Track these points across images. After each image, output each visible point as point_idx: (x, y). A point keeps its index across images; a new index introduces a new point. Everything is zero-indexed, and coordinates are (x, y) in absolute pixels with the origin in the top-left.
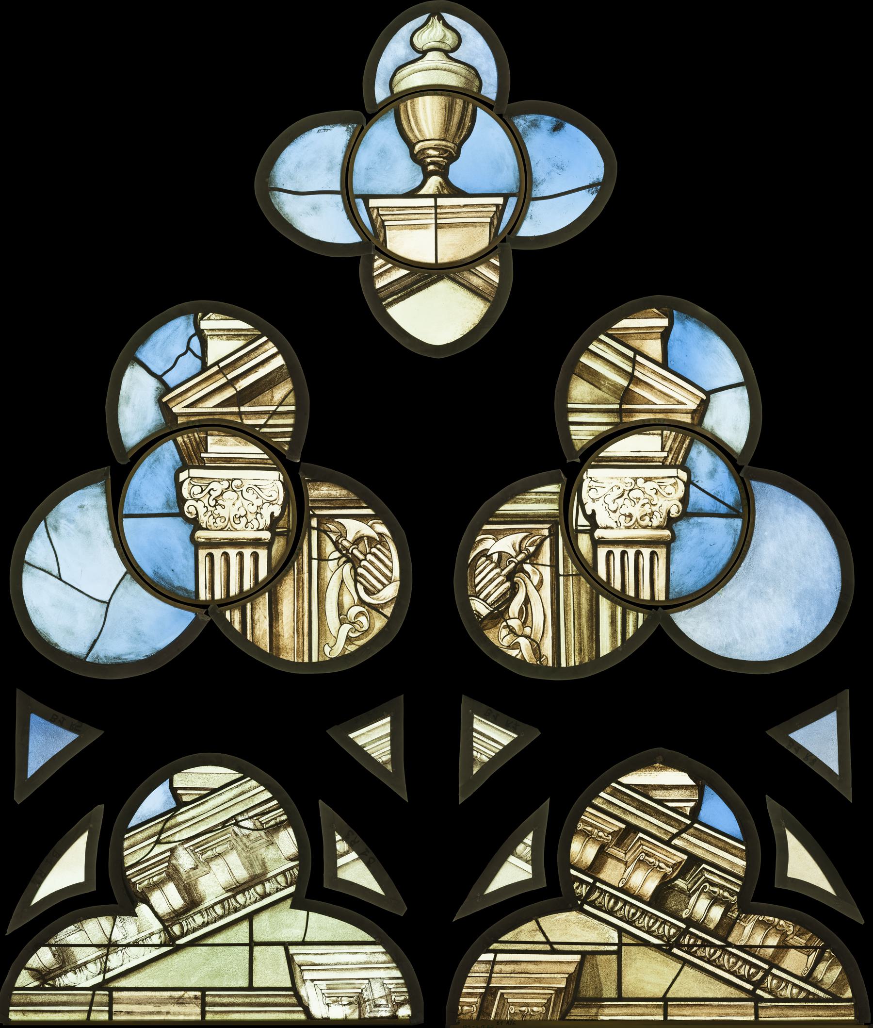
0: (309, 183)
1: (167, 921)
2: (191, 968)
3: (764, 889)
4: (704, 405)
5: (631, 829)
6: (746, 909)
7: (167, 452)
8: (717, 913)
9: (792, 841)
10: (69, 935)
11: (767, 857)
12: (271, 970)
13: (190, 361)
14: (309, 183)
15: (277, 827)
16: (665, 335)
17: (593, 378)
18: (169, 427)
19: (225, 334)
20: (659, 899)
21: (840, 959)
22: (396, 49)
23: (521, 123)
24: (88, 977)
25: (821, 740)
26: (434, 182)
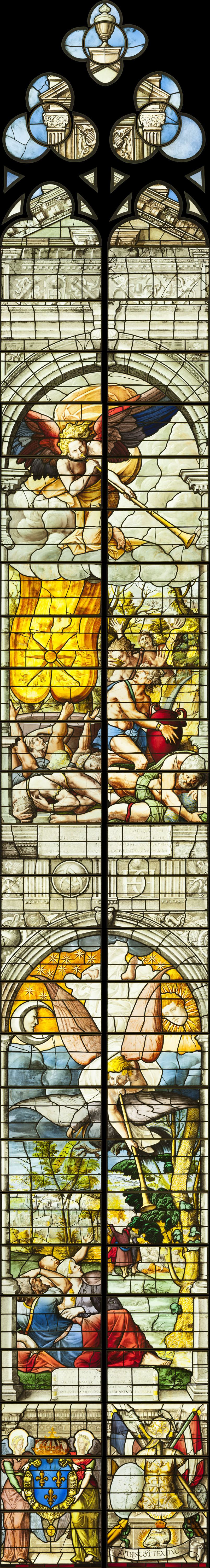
0: (74, 44)
1: (40, 222)
2: (46, 233)
3: (184, 214)
4: (169, 97)
5: (152, 199)
6: (179, 219)
7: (40, 109)
8: (172, 219)
9: (191, 202)
10: (17, 225)
11: (184, 206)
12: (65, 233)
13: (46, 87)
14: (74, 44)
15: (67, 199)
16: (160, 81)
17: (143, 91)
18: (41, 103)
19: (54, 80)
20: (159, 216)
21: (202, 230)
22: (95, 12)
23: (125, 30)
24: (21, 235)
25: (197, 178)
26: (104, 44)
